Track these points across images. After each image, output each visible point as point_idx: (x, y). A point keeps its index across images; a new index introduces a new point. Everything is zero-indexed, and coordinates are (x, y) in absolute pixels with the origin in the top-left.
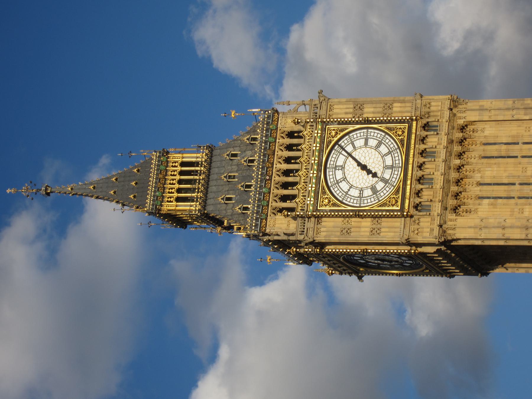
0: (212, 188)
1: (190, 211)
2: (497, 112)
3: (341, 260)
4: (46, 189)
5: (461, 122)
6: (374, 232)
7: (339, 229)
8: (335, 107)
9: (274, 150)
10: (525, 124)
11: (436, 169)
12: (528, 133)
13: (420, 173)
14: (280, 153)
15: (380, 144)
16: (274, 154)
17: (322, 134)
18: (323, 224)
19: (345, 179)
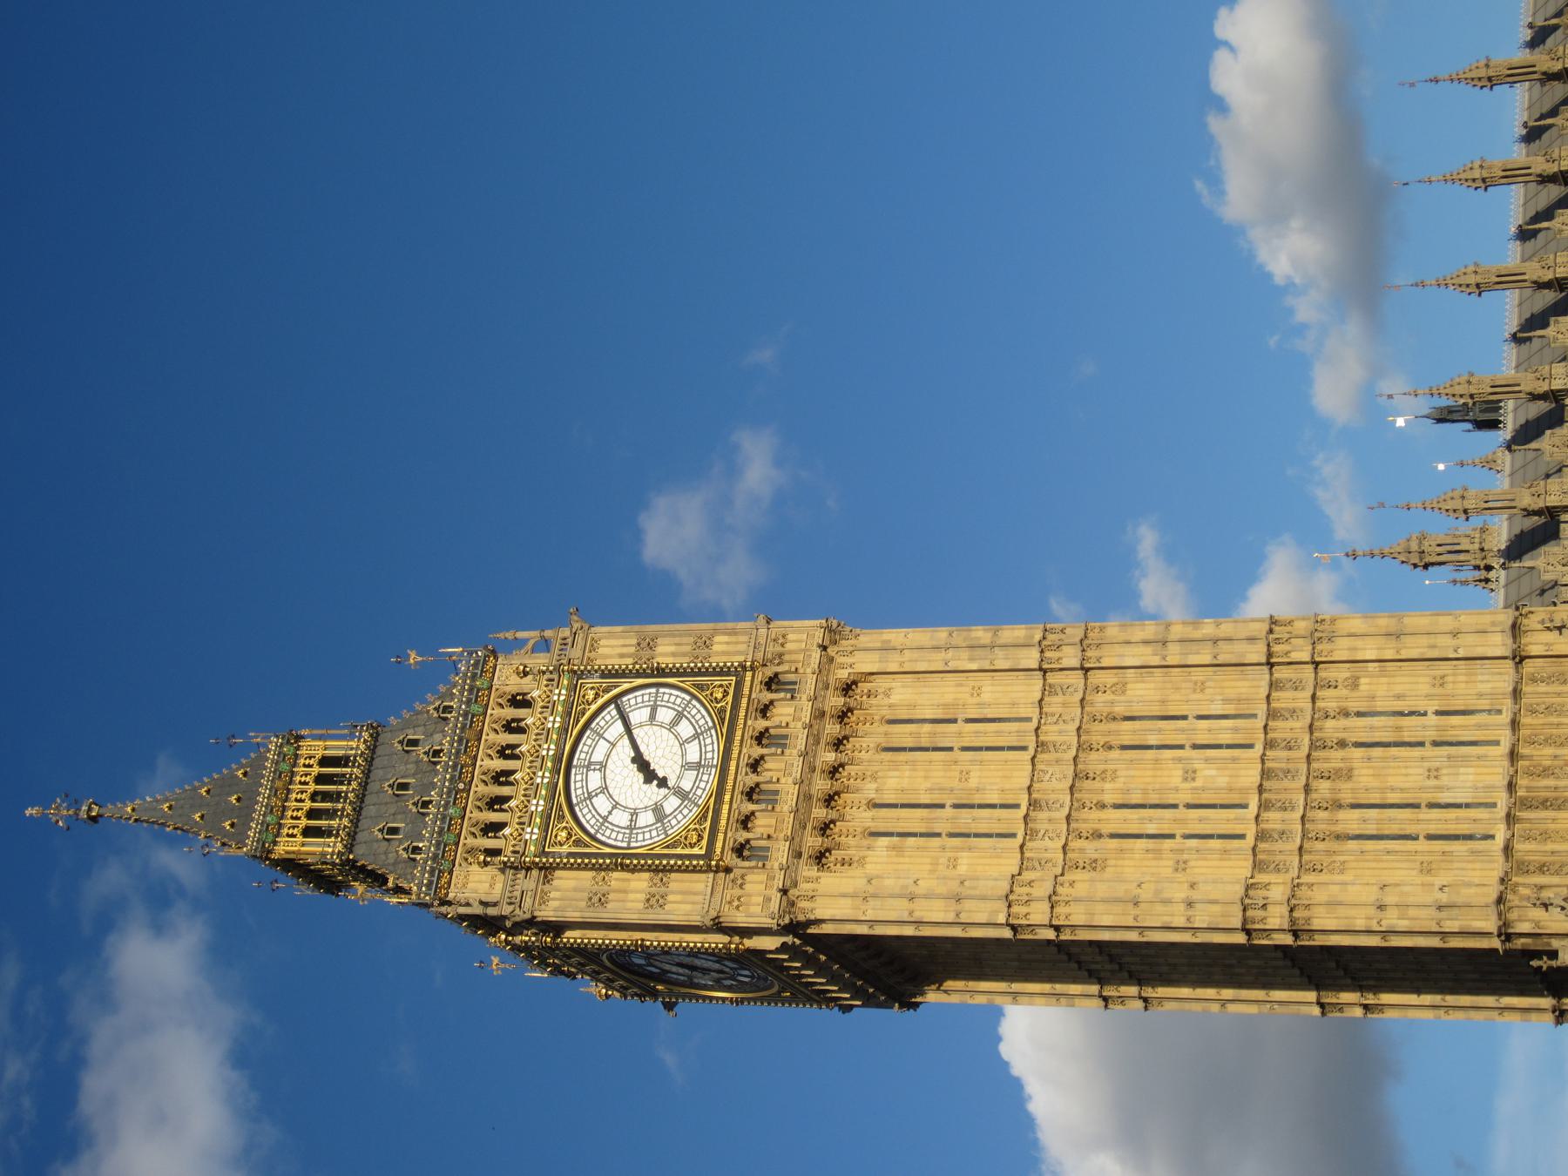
0: (370, 810)
1: (324, 854)
2: (916, 654)
3: (608, 964)
4: (90, 809)
5: (843, 674)
6: (653, 901)
7: (586, 895)
8: (602, 642)
9: (481, 731)
10: (973, 680)
11: (784, 771)
12: (975, 700)
13: (752, 779)
14: (492, 736)
15: (680, 716)
16: (479, 740)
17: (568, 696)
18: (555, 883)
19: (604, 789)
